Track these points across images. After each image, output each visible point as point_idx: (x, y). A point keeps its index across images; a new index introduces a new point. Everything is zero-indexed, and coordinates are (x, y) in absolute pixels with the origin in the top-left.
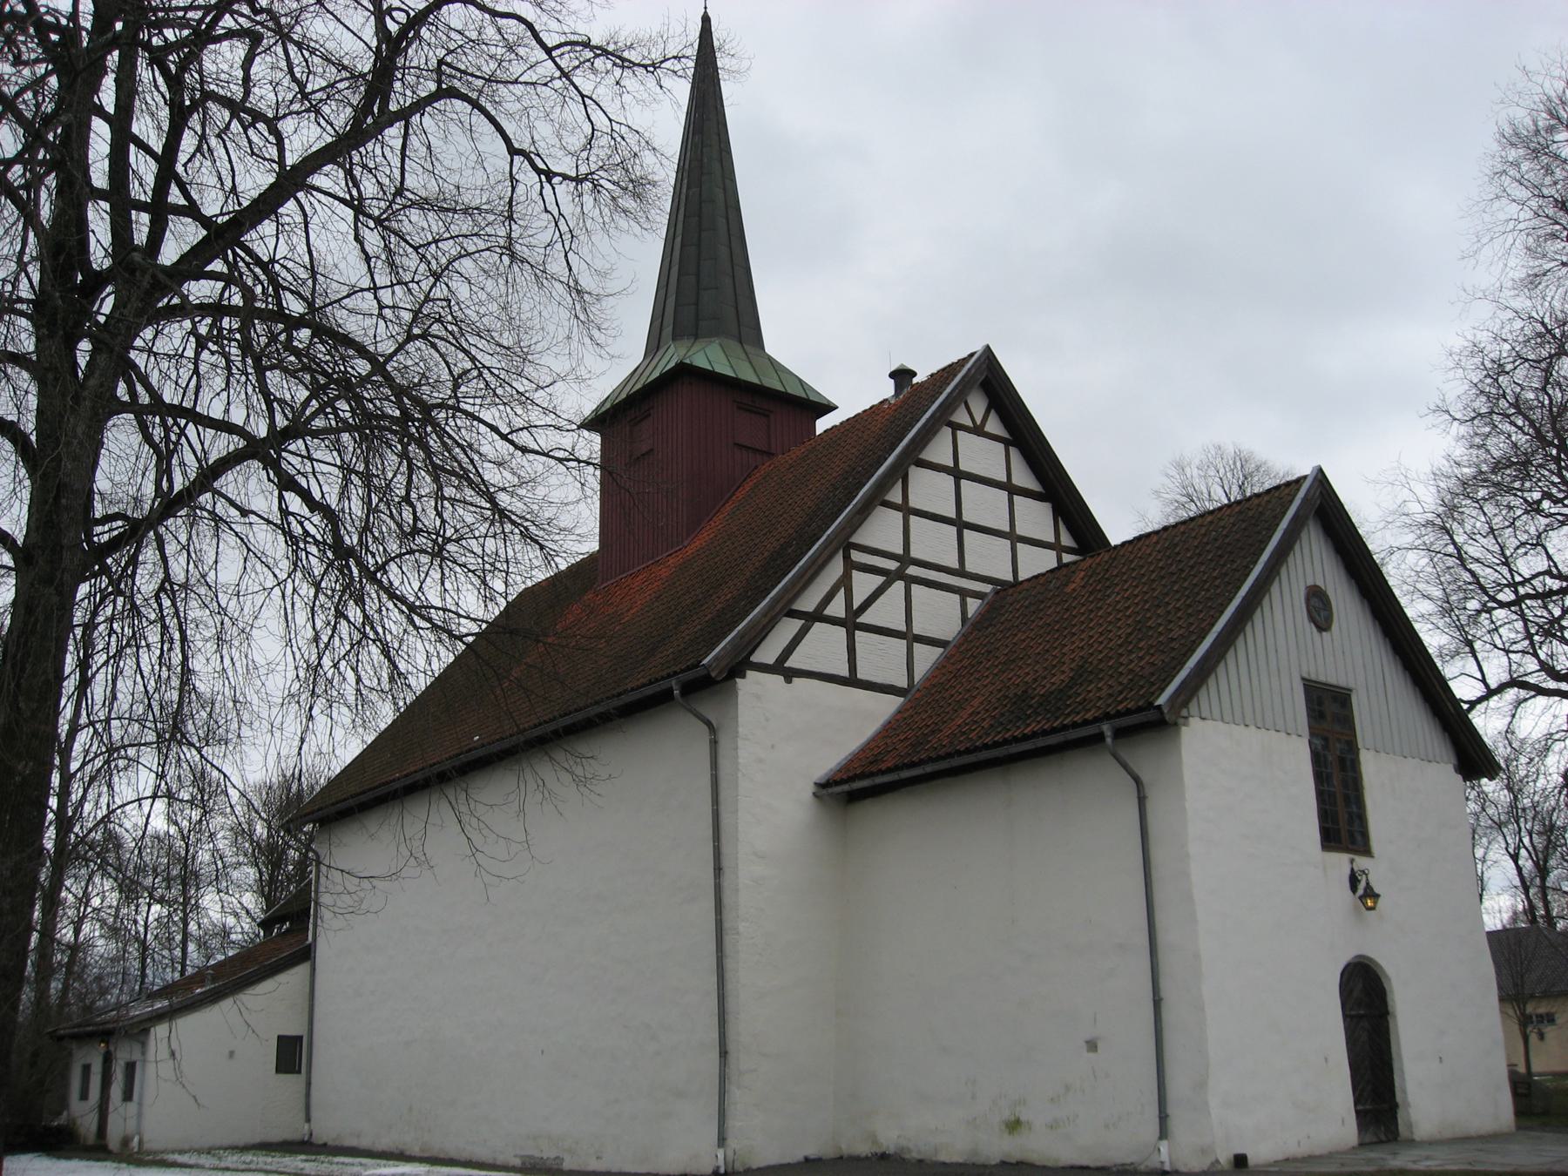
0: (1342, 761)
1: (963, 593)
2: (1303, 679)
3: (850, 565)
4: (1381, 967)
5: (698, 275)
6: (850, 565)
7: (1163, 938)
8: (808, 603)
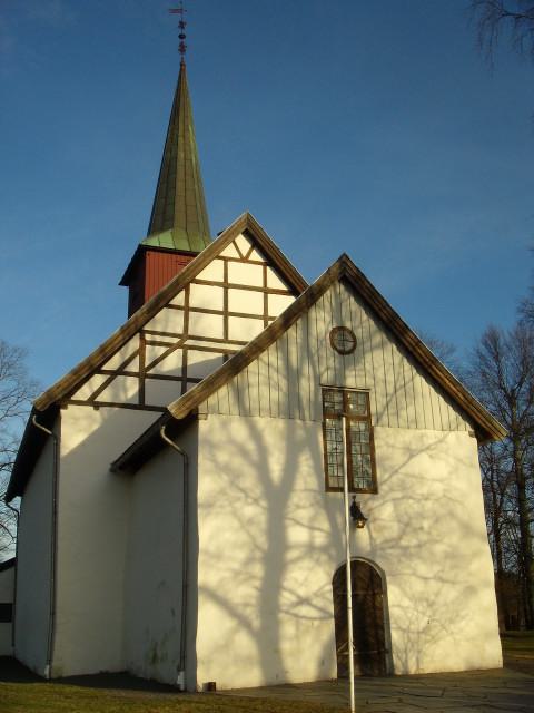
3: (144, 342)
6: (144, 342)
8: (113, 363)
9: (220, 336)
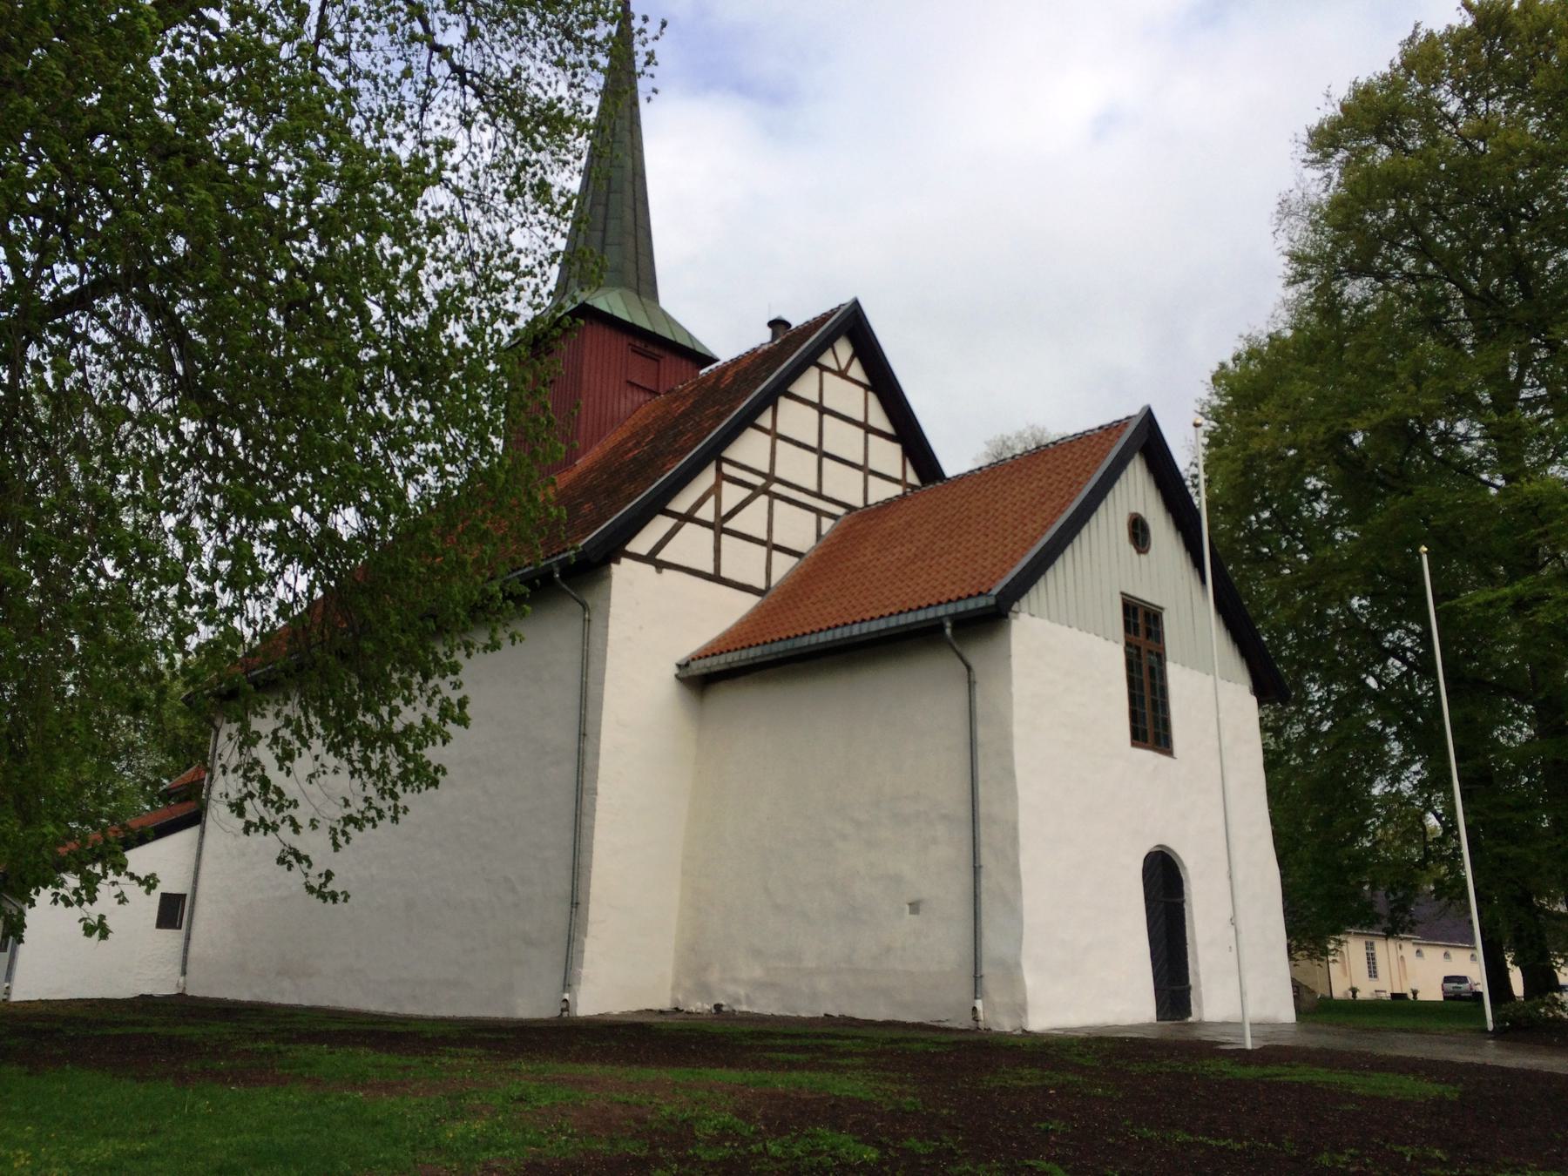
0: (1152, 669)
1: (820, 513)
2: (1122, 593)
3: (721, 476)
4: (1178, 857)
5: (604, 231)
7: (983, 809)
8: (681, 504)
9: (813, 487)
